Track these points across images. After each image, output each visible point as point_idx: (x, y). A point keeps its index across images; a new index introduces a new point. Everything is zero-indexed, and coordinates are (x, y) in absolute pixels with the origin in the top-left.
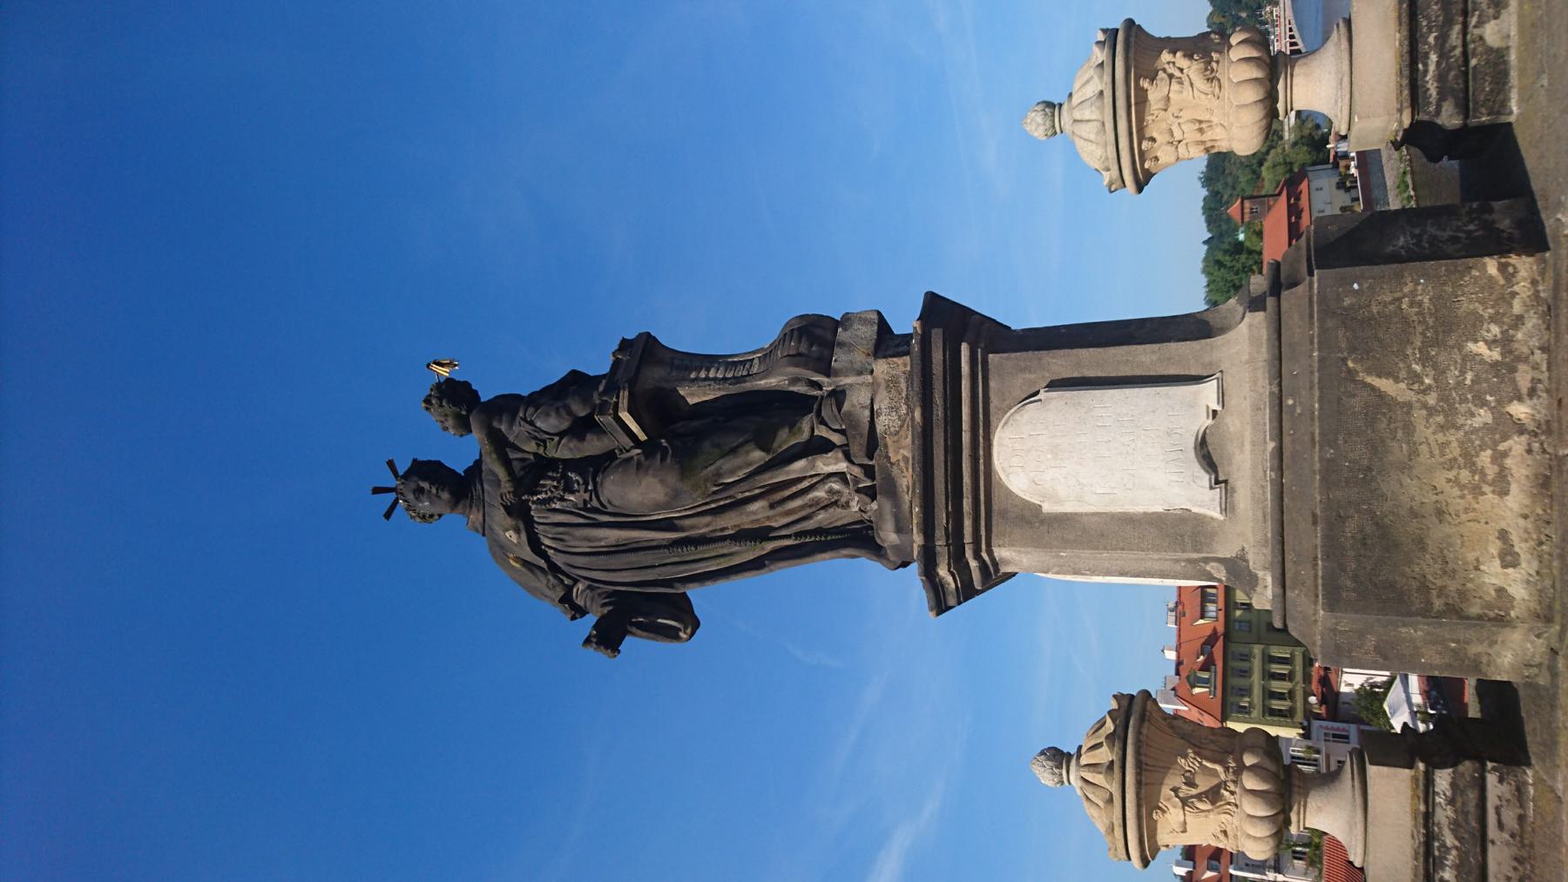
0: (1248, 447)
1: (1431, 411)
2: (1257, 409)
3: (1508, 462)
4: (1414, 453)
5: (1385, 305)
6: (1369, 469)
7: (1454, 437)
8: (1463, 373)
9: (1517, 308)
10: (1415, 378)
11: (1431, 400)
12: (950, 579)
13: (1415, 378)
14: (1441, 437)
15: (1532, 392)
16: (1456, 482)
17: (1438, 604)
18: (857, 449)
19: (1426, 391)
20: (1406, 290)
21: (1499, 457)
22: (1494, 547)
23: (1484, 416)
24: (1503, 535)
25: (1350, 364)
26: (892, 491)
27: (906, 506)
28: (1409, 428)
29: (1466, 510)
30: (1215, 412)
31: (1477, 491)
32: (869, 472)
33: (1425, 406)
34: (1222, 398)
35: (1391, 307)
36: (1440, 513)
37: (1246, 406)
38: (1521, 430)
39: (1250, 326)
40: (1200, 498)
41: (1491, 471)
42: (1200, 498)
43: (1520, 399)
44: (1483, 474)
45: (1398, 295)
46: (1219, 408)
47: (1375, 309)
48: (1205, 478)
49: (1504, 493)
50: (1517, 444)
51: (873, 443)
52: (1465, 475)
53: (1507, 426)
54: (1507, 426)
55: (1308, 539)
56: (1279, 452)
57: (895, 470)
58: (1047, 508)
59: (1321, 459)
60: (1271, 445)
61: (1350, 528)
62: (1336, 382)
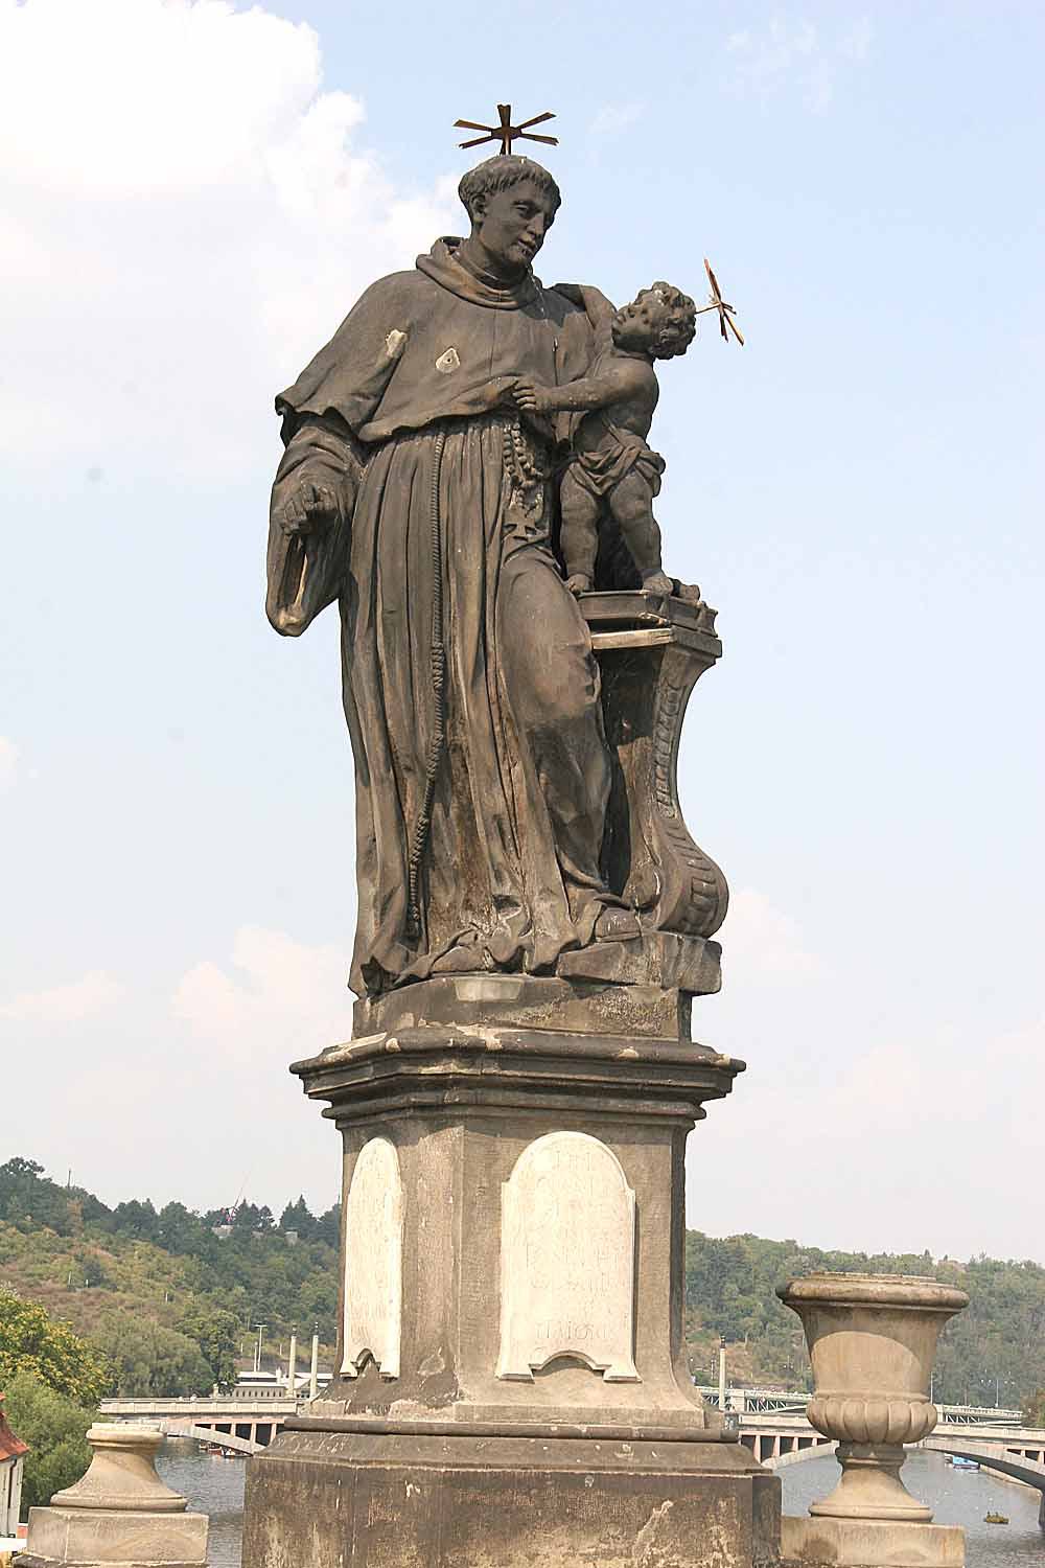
0: (576, 1405)
2: (614, 1414)
5: (717, 1537)
6: (574, 1518)
12: (437, 1069)
18: (579, 963)
20: (729, 1556)
26: (527, 997)
27: (510, 1017)
30: (602, 1372)
32: (545, 970)
34: (616, 1381)
35: (715, 1543)
39: (692, 1413)
40: (517, 1352)
42: (517, 1352)
45: (725, 1548)
46: (607, 1376)
47: (714, 1528)
48: (541, 1359)
51: (583, 985)
55: (508, 1458)
56: (578, 1436)
57: (550, 1007)
58: (510, 1191)
59: (584, 1475)
60: (584, 1429)
61: (520, 1499)
62: (650, 1487)
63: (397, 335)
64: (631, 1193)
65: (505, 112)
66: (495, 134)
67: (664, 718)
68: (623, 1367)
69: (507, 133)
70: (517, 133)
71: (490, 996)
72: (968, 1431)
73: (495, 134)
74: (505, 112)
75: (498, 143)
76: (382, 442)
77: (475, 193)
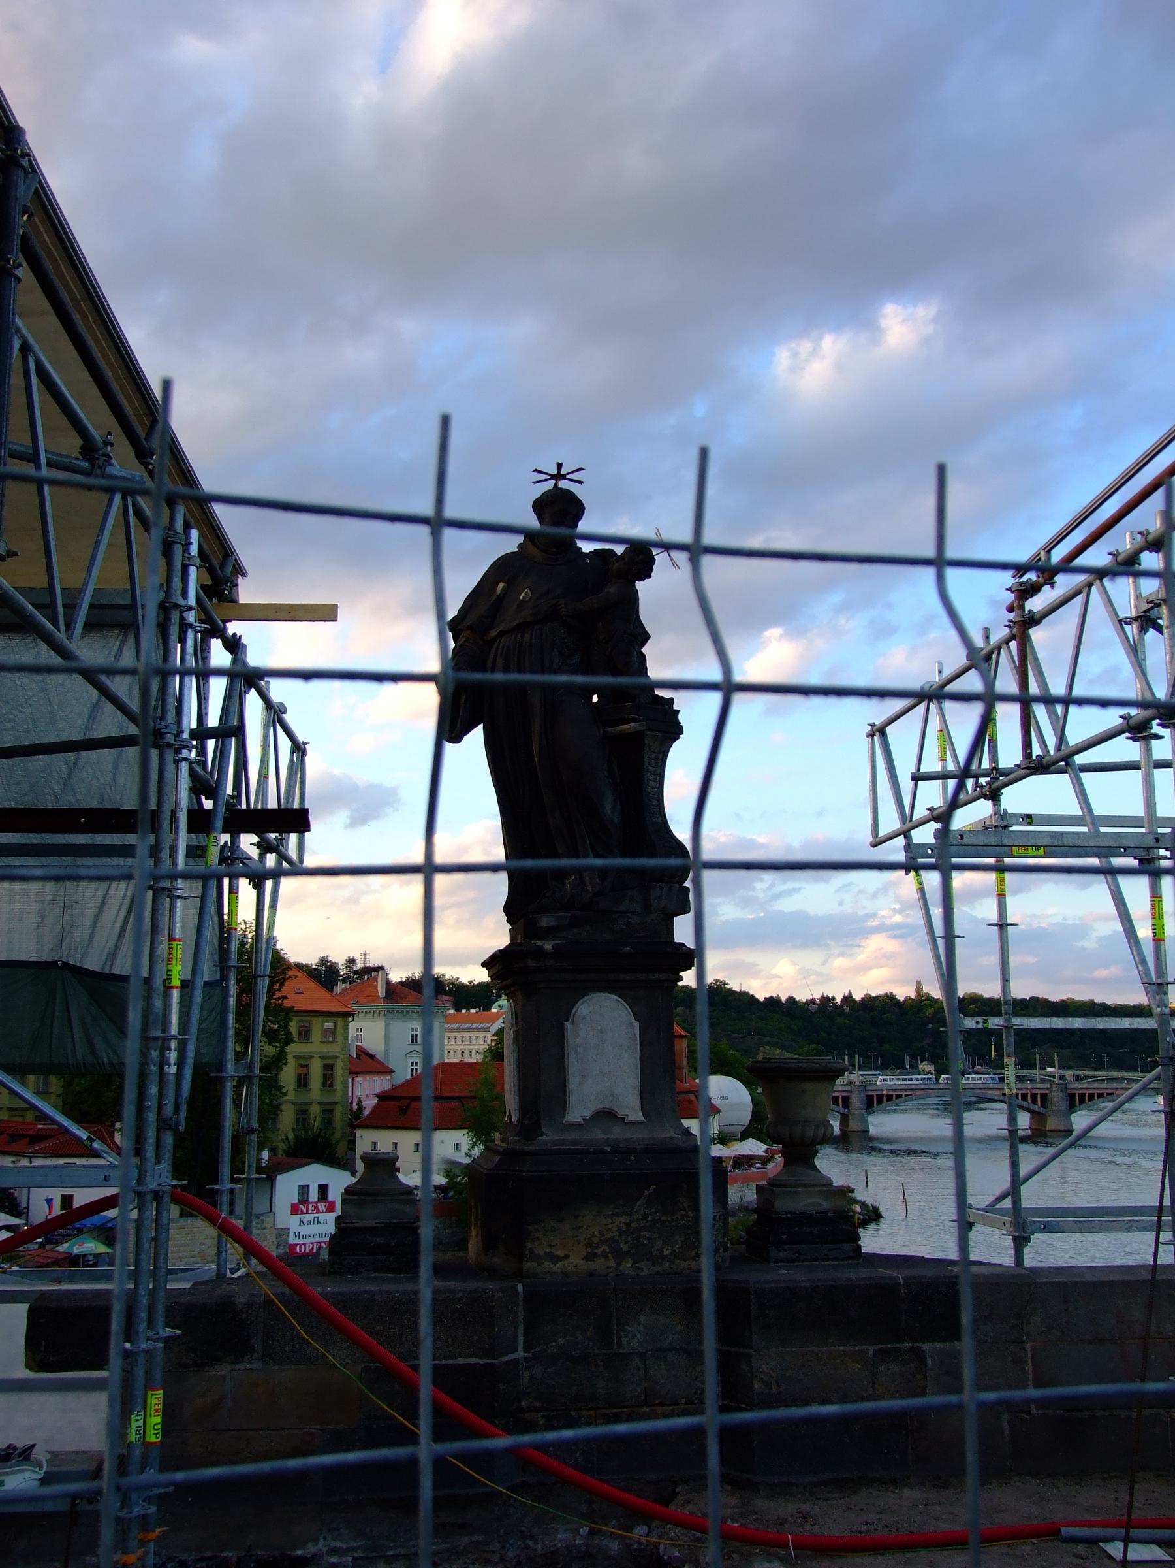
0: (606, 1137)
1: (628, 1225)
2: (628, 1140)
3: (602, 1260)
4: (607, 1217)
7: (616, 1234)
8: (647, 1238)
9: (677, 1261)
10: (645, 1217)
11: (634, 1225)
13: (645, 1217)
14: (615, 1229)
15: (638, 1268)
16: (593, 1236)
17: (530, 1228)
19: (639, 1221)
21: (605, 1255)
22: (560, 1253)
23: (625, 1248)
24: (567, 1257)
25: (653, 1187)
28: (619, 1215)
29: (579, 1242)
31: (589, 1245)
33: (631, 1221)
36: (577, 1229)
37: (628, 1136)
38: (619, 1264)
41: (599, 1251)
43: (634, 1263)
44: (597, 1248)
49: (586, 1259)
50: (612, 1264)
52: (596, 1240)
53: (620, 1256)
54: (620, 1256)
63: (501, 585)
64: (637, 1024)
65: (559, 466)
66: (553, 477)
67: (651, 769)
68: (636, 1115)
69: (558, 477)
70: (563, 477)
71: (552, 923)
72: (1115, 1085)
73: (553, 477)
74: (559, 466)
75: (553, 482)
76: (494, 640)
77: (541, 506)
